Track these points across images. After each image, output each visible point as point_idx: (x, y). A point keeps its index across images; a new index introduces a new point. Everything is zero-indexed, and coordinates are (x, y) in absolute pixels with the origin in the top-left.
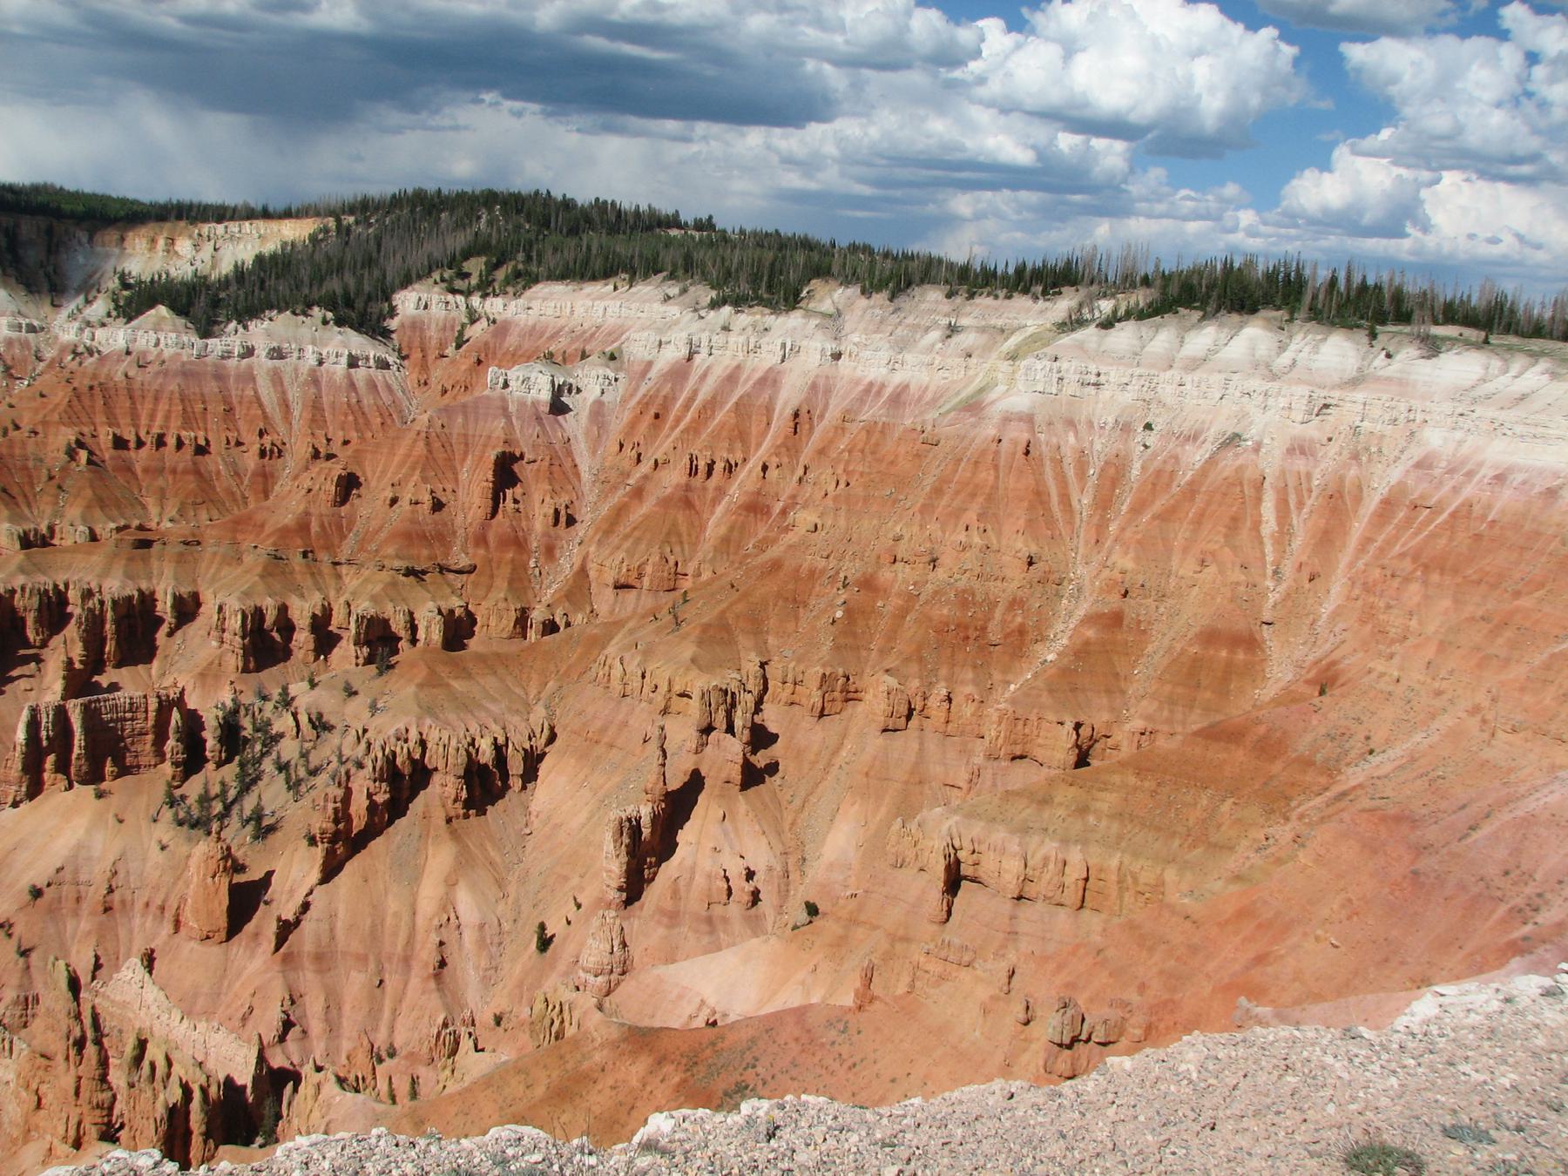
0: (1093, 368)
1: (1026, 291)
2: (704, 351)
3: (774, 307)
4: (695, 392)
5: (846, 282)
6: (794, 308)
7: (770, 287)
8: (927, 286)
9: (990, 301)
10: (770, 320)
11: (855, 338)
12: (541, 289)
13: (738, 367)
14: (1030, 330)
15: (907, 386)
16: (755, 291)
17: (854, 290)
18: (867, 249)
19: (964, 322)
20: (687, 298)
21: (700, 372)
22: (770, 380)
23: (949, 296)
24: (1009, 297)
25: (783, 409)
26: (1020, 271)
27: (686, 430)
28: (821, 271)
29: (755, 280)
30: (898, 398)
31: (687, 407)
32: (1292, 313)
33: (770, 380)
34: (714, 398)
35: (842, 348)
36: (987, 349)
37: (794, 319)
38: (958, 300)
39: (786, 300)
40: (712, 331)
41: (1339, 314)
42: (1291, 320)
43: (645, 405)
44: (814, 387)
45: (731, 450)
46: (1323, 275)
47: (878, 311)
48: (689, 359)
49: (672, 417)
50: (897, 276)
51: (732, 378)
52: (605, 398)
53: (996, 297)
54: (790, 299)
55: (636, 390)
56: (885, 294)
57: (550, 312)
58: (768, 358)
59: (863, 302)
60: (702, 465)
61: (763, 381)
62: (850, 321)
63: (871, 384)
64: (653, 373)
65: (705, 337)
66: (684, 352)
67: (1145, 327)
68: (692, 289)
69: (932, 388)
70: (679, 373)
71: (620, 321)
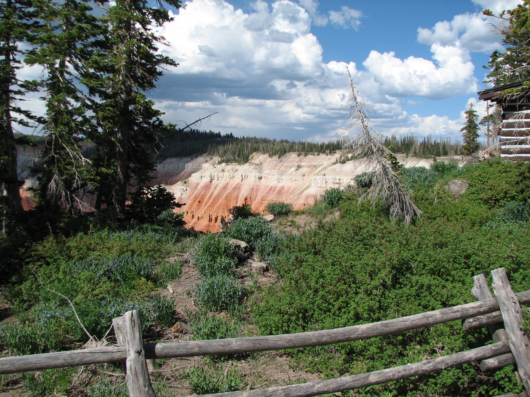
0: (338, 178)
1: (324, 152)
2: (216, 179)
3: (239, 163)
4: (213, 193)
5: (264, 153)
6: (246, 162)
7: (239, 156)
8: (291, 153)
9: (312, 156)
10: (238, 167)
11: (267, 172)
12: (168, 160)
13: (227, 184)
14: (324, 166)
15: (283, 187)
16: (234, 158)
17: (267, 155)
18: (287, 141)
19: (303, 164)
20: (212, 161)
21: (215, 186)
22: (237, 188)
23: (298, 156)
24: (318, 155)
25: (242, 197)
26: (322, 146)
27: (209, 206)
28: (256, 150)
29: (234, 153)
30: (280, 192)
31: (210, 198)
32: (407, 154)
33: (237, 188)
34: (219, 195)
35: (262, 175)
36: (310, 173)
37: (246, 166)
38: (302, 157)
39: (243, 160)
40: (218, 172)
41: (424, 153)
42: (407, 157)
43: (195, 198)
44: (252, 189)
45: (224, 212)
46: (420, 140)
47: (275, 162)
48: (211, 182)
49: (205, 202)
50: (280, 149)
51: (225, 188)
52: (182, 196)
53: (314, 155)
54: (246, 160)
55: (193, 193)
56: (277, 156)
57: (171, 168)
58: (237, 180)
59: (270, 159)
60: (213, 218)
61: (235, 188)
62: (265, 166)
63: (272, 187)
64: (199, 187)
65: (216, 174)
66: (209, 179)
67: (357, 163)
68: (214, 158)
69: (292, 188)
70: (207, 187)
71: (192, 170)
